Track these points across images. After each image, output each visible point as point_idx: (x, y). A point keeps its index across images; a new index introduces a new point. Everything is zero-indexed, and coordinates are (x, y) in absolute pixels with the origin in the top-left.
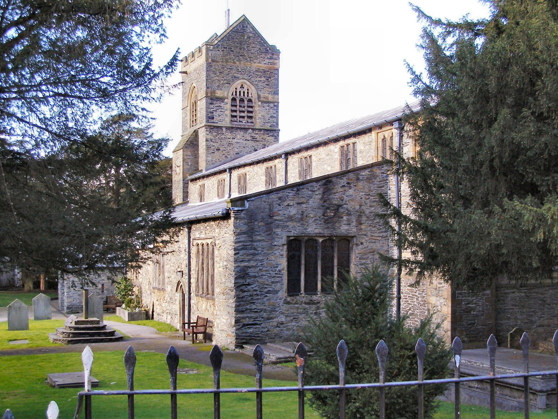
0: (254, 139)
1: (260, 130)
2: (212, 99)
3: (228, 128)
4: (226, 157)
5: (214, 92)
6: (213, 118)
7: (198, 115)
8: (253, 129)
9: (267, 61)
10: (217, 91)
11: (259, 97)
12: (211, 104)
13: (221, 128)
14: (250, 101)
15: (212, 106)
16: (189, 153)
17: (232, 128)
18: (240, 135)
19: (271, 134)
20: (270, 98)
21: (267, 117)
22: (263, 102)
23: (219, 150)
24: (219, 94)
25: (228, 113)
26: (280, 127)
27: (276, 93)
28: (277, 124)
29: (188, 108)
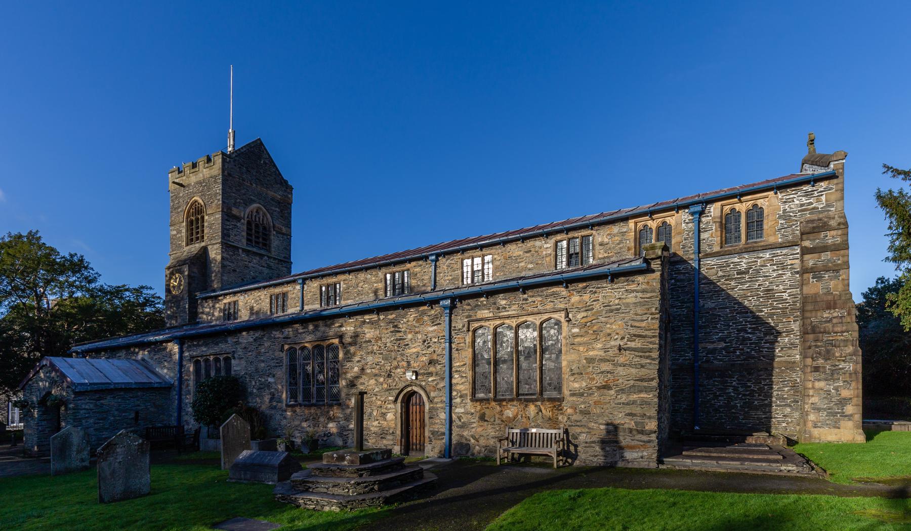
0: (269, 267)
1: (275, 259)
11: (274, 226)
13: (237, 248)
14: (264, 228)
16: (195, 270)
17: (249, 251)
18: (256, 260)
19: (284, 265)
20: (284, 230)
22: (278, 232)
23: (234, 271)
25: (244, 234)
27: (289, 225)
28: (290, 256)
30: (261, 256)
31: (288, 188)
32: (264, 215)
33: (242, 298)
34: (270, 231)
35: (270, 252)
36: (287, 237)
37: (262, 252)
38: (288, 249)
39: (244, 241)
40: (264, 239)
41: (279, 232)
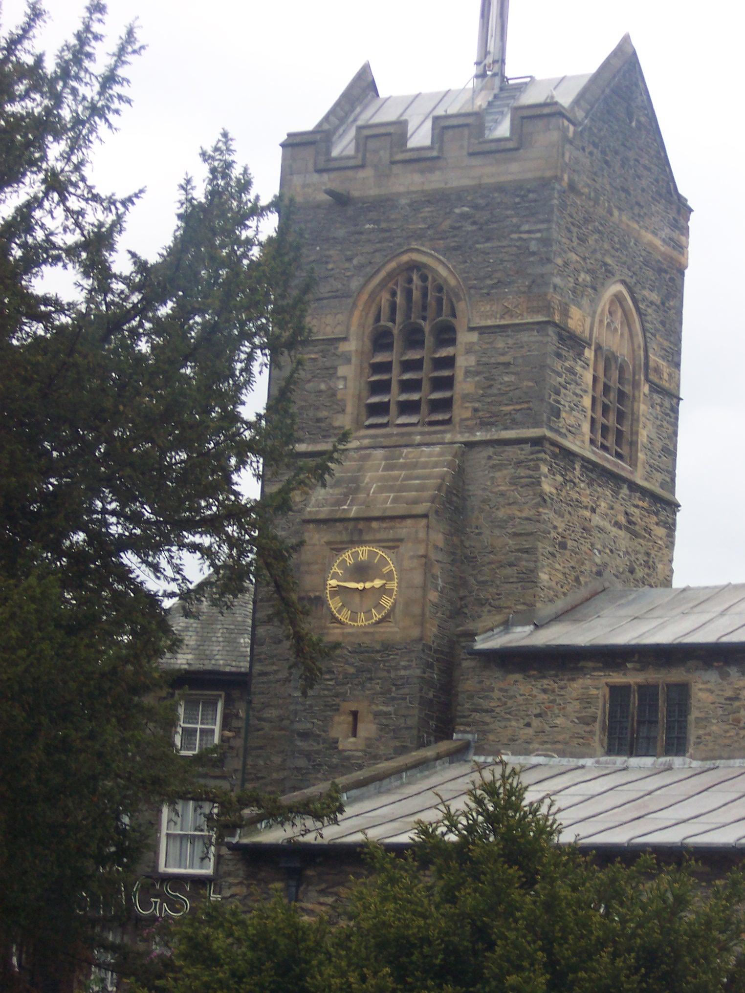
0: (630, 527)
2: (561, 338)
3: (590, 466)
4: (577, 579)
5: (565, 313)
6: (558, 416)
7: (464, 386)
8: (634, 487)
9: (666, 232)
10: (575, 312)
12: (559, 356)
13: (568, 455)
15: (558, 365)
21: (658, 445)
23: (563, 546)
24: (577, 320)
25: (587, 402)
26: (681, 495)
27: (674, 357)
29: (351, 346)
30: (615, 479)
31: (680, 209)
32: (626, 314)
33: (712, 677)
34: (636, 385)
35: (633, 463)
36: (669, 397)
37: (622, 468)
38: (670, 452)
39: (586, 427)
40: (621, 416)
41: (656, 389)
